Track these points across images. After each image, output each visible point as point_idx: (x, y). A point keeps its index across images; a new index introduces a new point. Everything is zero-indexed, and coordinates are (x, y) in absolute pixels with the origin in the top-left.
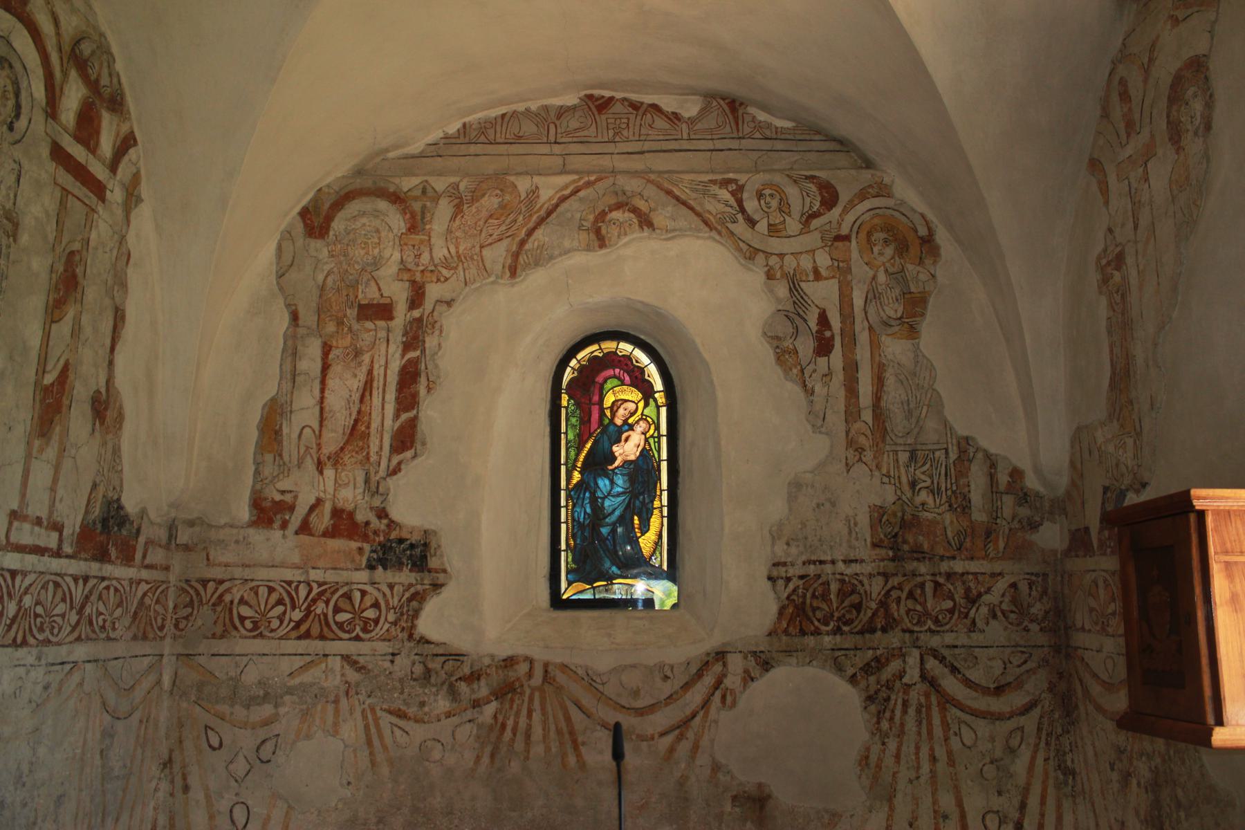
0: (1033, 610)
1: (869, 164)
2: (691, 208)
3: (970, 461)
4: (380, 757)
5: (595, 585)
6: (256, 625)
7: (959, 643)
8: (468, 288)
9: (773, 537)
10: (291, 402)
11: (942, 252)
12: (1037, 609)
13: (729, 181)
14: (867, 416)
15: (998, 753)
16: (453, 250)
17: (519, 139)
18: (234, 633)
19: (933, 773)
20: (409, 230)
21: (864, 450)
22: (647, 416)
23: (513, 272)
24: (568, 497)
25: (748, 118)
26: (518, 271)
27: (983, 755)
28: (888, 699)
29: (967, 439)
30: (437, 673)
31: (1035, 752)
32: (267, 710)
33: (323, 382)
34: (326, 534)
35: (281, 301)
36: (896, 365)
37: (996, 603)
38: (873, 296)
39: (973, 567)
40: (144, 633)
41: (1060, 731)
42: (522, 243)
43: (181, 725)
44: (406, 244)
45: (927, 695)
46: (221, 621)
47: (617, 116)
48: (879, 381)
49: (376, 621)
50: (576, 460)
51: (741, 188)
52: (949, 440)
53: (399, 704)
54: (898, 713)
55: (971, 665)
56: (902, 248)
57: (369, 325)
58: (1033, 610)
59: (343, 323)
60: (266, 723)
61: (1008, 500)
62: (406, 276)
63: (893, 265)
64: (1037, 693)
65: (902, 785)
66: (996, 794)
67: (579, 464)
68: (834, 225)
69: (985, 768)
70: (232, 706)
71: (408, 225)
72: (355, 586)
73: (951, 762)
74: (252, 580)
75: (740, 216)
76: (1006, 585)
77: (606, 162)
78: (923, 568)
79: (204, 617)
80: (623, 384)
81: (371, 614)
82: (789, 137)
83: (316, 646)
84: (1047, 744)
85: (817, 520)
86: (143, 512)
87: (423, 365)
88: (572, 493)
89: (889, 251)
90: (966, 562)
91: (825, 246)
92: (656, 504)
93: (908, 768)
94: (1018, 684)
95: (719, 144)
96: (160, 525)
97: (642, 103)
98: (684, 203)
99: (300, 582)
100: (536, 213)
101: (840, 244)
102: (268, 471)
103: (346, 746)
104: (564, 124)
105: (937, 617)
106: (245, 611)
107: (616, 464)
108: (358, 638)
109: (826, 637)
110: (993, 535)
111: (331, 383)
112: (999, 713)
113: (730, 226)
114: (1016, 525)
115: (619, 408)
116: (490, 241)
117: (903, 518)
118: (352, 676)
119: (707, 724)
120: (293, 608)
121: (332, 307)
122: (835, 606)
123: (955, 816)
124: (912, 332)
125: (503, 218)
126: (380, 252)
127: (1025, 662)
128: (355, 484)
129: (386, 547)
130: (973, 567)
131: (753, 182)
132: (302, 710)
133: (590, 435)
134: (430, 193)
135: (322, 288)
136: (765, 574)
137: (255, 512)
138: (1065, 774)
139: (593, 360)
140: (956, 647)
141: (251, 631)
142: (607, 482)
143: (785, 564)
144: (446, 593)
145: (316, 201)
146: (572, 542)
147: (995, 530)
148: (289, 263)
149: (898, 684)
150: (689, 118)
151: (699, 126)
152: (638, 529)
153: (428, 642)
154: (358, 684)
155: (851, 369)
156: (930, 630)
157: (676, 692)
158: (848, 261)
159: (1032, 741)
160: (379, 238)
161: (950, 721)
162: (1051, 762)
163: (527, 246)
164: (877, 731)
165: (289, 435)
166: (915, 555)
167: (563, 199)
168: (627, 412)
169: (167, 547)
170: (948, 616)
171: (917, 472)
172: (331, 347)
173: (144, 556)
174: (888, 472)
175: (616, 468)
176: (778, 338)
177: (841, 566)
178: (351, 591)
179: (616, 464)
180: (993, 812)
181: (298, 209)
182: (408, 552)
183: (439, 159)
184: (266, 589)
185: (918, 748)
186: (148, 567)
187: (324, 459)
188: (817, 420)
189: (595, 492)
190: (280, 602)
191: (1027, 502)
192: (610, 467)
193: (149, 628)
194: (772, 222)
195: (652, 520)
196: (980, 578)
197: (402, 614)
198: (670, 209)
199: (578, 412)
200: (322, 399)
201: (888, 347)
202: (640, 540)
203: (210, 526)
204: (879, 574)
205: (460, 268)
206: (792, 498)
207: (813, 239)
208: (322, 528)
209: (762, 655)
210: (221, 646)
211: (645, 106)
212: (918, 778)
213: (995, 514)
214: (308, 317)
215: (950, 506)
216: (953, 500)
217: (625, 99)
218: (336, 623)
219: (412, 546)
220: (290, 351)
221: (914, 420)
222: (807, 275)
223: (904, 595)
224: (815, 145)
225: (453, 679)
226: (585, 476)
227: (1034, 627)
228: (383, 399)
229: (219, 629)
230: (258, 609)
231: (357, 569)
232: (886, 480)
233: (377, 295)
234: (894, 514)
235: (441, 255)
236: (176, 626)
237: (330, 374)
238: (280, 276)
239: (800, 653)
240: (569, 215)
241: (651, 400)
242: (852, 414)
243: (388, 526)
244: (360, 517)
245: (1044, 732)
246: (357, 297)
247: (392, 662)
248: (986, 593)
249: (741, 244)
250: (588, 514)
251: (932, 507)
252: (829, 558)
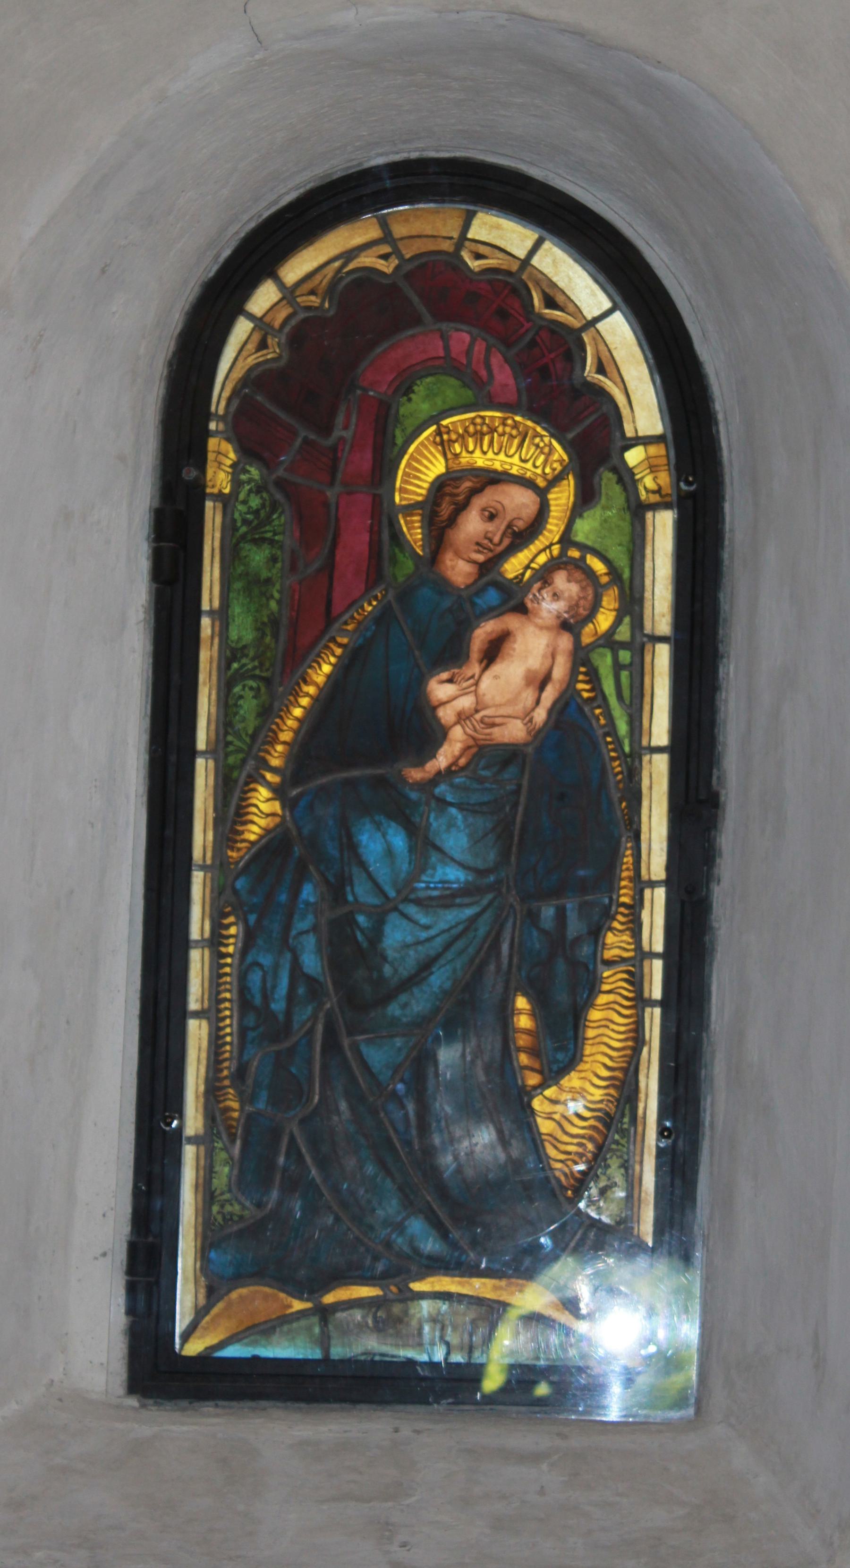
5: (329, 1299)
22: (585, 548)
67: (276, 757)
88: (240, 884)
107: (442, 760)
115: (462, 507)
142: (399, 840)
152: (534, 1052)
168: (496, 529)
175: (440, 776)
179: (442, 760)
192: (416, 775)
195: (595, 1015)
202: (537, 1104)
241: (607, 480)
250: (311, 980)
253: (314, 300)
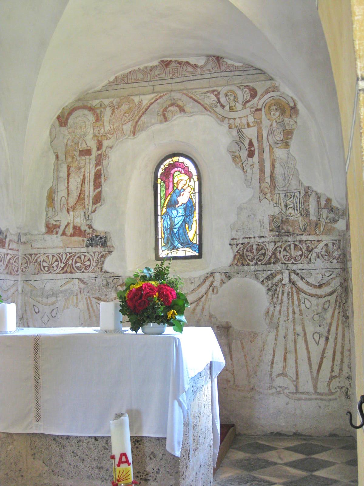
0: (334, 254)
1: (271, 79)
2: (199, 103)
4: (92, 314)
5: (172, 251)
6: (49, 269)
7: (304, 268)
8: (118, 141)
9: (231, 229)
10: (57, 188)
11: (300, 112)
12: (336, 254)
13: (214, 91)
14: (268, 180)
15: (320, 310)
16: (112, 127)
17: (136, 81)
18: (42, 272)
19: (294, 319)
20: (96, 121)
21: (266, 193)
23: (134, 134)
24: (162, 218)
25: (224, 63)
26: (136, 133)
27: (314, 311)
28: (276, 290)
29: (308, 187)
30: (111, 283)
31: (334, 310)
32: (54, 299)
33: (68, 180)
34: (71, 236)
35: (52, 151)
36: (280, 160)
37: (319, 252)
38: (271, 132)
39: (311, 238)
40: (11, 272)
41: (344, 301)
42: (137, 122)
43: (26, 305)
44: (95, 126)
45: (292, 288)
46: (37, 269)
47: (173, 68)
48: (273, 166)
49: (89, 266)
50: (164, 204)
51: (219, 93)
52: (301, 188)
53: (98, 295)
54: (280, 295)
55: (309, 276)
56: (283, 112)
57: (83, 158)
58: (334, 254)
59: (74, 158)
60: (54, 303)
61: (325, 211)
62: (95, 138)
63: (279, 119)
65: (281, 323)
66: (318, 326)
67: (165, 205)
68: (255, 105)
69: (315, 316)
70: (42, 298)
71: (96, 119)
72: (82, 254)
73: (301, 314)
74: (47, 253)
75: (218, 105)
76: (323, 245)
77: (169, 87)
78: (290, 239)
79: (32, 267)
80: (181, 173)
81: (87, 263)
82: (240, 70)
83: (69, 275)
84: (339, 307)
85: (248, 222)
86: (7, 230)
87: (103, 171)
88: (163, 217)
89: (277, 114)
90: (307, 236)
91: (252, 114)
92: (194, 219)
93: (284, 316)
94: (328, 283)
95: (213, 75)
96: (14, 235)
97: (182, 62)
98: (197, 101)
99: (63, 253)
100: (141, 110)
101: (258, 112)
102: (51, 213)
103: (81, 311)
104: (153, 73)
105: (295, 258)
106: (45, 264)
108: (83, 272)
109: (252, 266)
110: (318, 225)
111: (71, 180)
112: (320, 295)
113: (214, 109)
114: (328, 221)
116: (125, 122)
117: (282, 220)
118: (82, 285)
119: (208, 300)
120: (61, 262)
121: (70, 152)
122: (255, 254)
123: (302, 334)
124: (287, 145)
125: (130, 113)
126: (86, 130)
127: (331, 275)
128: (80, 217)
129: (92, 239)
130: (311, 238)
131: (223, 90)
132: (65, 298)
133: (169, 194)
134: (103, 106)
135: (66, 145)
136: (229, 243)
137: (47, 229)
138: (346, 319)
139: (170, 165)
140: (303, 269)
141: (47, 271)
142: (176, 212)
143: (236, 239)
144: (113, 254)
145: (62, 113)
146: (163, 235)
147: (319, 223)
148: (54, 137)
149: (280, 284)
150: (201, 66)
151: (204, 69)
153: (107, 272)
154: (84, 289)
155: (262, 162)
156: (293, 263)
157: (196, 288)
158: (261, 119)
159: (333, 306)
160: (86, 125)
161: (301, 298)
162: (341, 314)
163: (139, 123)
164: (272, 302)
165: (57, 200)
166: (287, 234)
167: (152, 103)
169: (18, 243)
170: (300, 257)
171: (288, 201)
172: (70, 167)
173: (9, 246)
174: (276, 202)
176: (233, 152)
177: (257, 239)
178: (81, 255)
180: (317, 333)
181: (56, 116)
182: (100, 240)
183: (107, 91)
184: (52, 256)
185: (288, 308)
186: (10, 249)
187: (69, 208)
188: (249, 183)
189: (171, 215)
190: (57, 261)
191: (332, 211)
192: (177, 206)
193: (12, 271)
194: (231, 106)
196: (313, 242)
197: (98, 263)
198: (191, 104)
199: (165, 185)
200: (68, 186)
201: (276, 152)
203: (32, 235)
204: (272, 242)
205: (115, 134)
206: (239, 214)
207: (247, 111)
208: (70, 233)
209: (227, 274)
210: (37, 277)
211: (184, 63)
212: (288, 320)
213: (319, 217)
214: (62, 157)
215: (301, 214)
216: (302, 212)
217: (176, 61)
218: (76, 267)
219: (101, 238)
220: (56, 170)
221: (286, 181)
222: (244, 126)
223: (282, 250)
224: (251, 72)
225: (117, 285)
226: (167, 210)
227: (335, 261)
228: (89, 185)
229: (36, 271)
230: (49, 263)
231: (82, 247)
232: (275, 205)
233: (85, 146)
234: (279, 218)
235: (107, 129)
236: (22, 271)
237: (70, 177)
238: (51, 142)
239: (242, 273)
240: (153, 110)
241: (192, 179)
242: (262, 179)
243: (93, 231)
244: (83, 229)
245: (338, 302)
246: (78, 147)
247: (95, 280)
248: (315, 248)
249: (219, 116)
251: (295, 216)
252: (253, 236)
253: (166, 166)
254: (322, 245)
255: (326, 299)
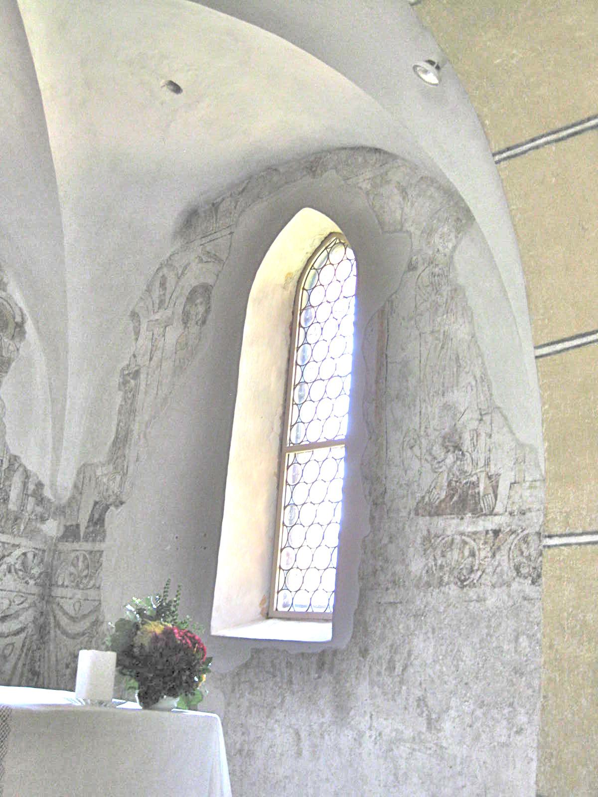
3: (15, 471)
12: (36, 571)
29: (15, 456)
37: (13, 563)
41: (35, 647)
61: (31, 500)
64: (26, 623)
76: (20, 553)
84: (26, 655)
94: (17, 615)
110: (18, 521)
114: (33, 517)
127: (22, 603)
159: (18, 652)
162: (27, 667)
196: (6, 546)
227: (32, 582)
248: (8, 556)
254: (18, 552)
255: (8, 640)
